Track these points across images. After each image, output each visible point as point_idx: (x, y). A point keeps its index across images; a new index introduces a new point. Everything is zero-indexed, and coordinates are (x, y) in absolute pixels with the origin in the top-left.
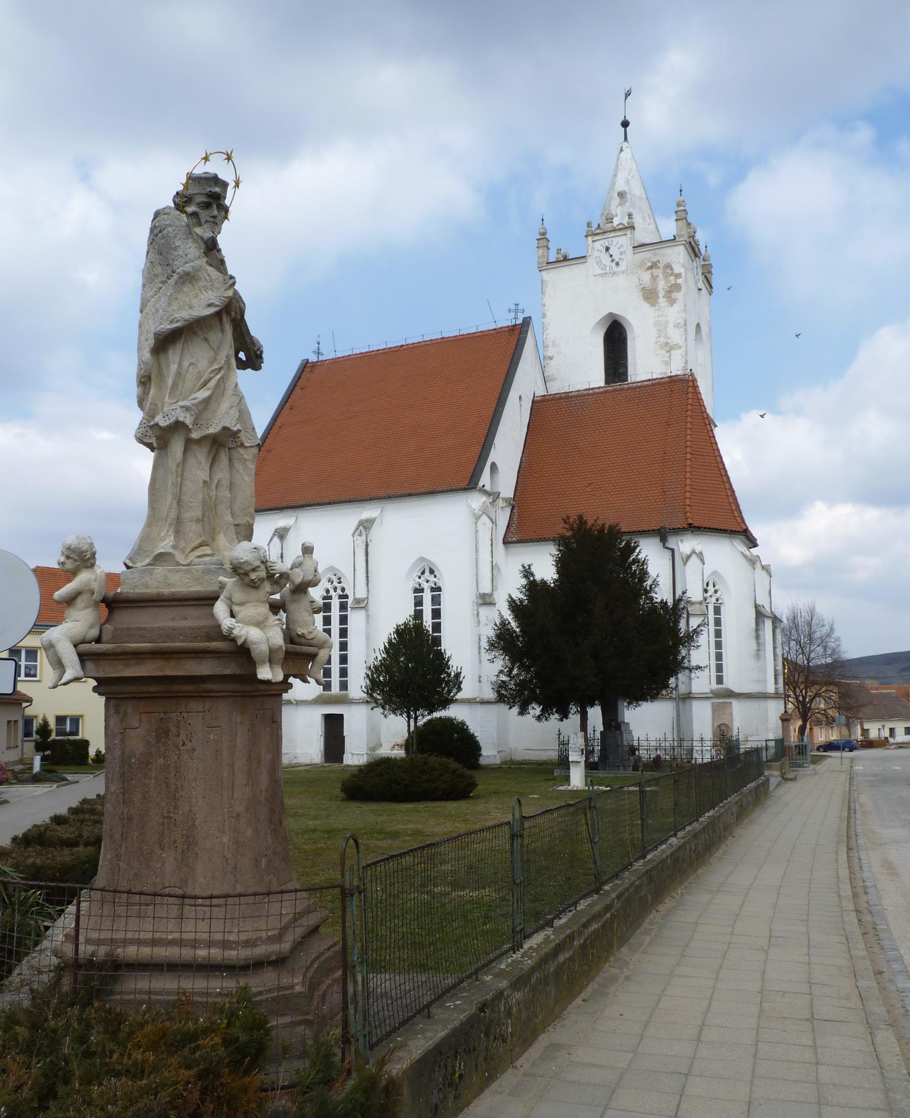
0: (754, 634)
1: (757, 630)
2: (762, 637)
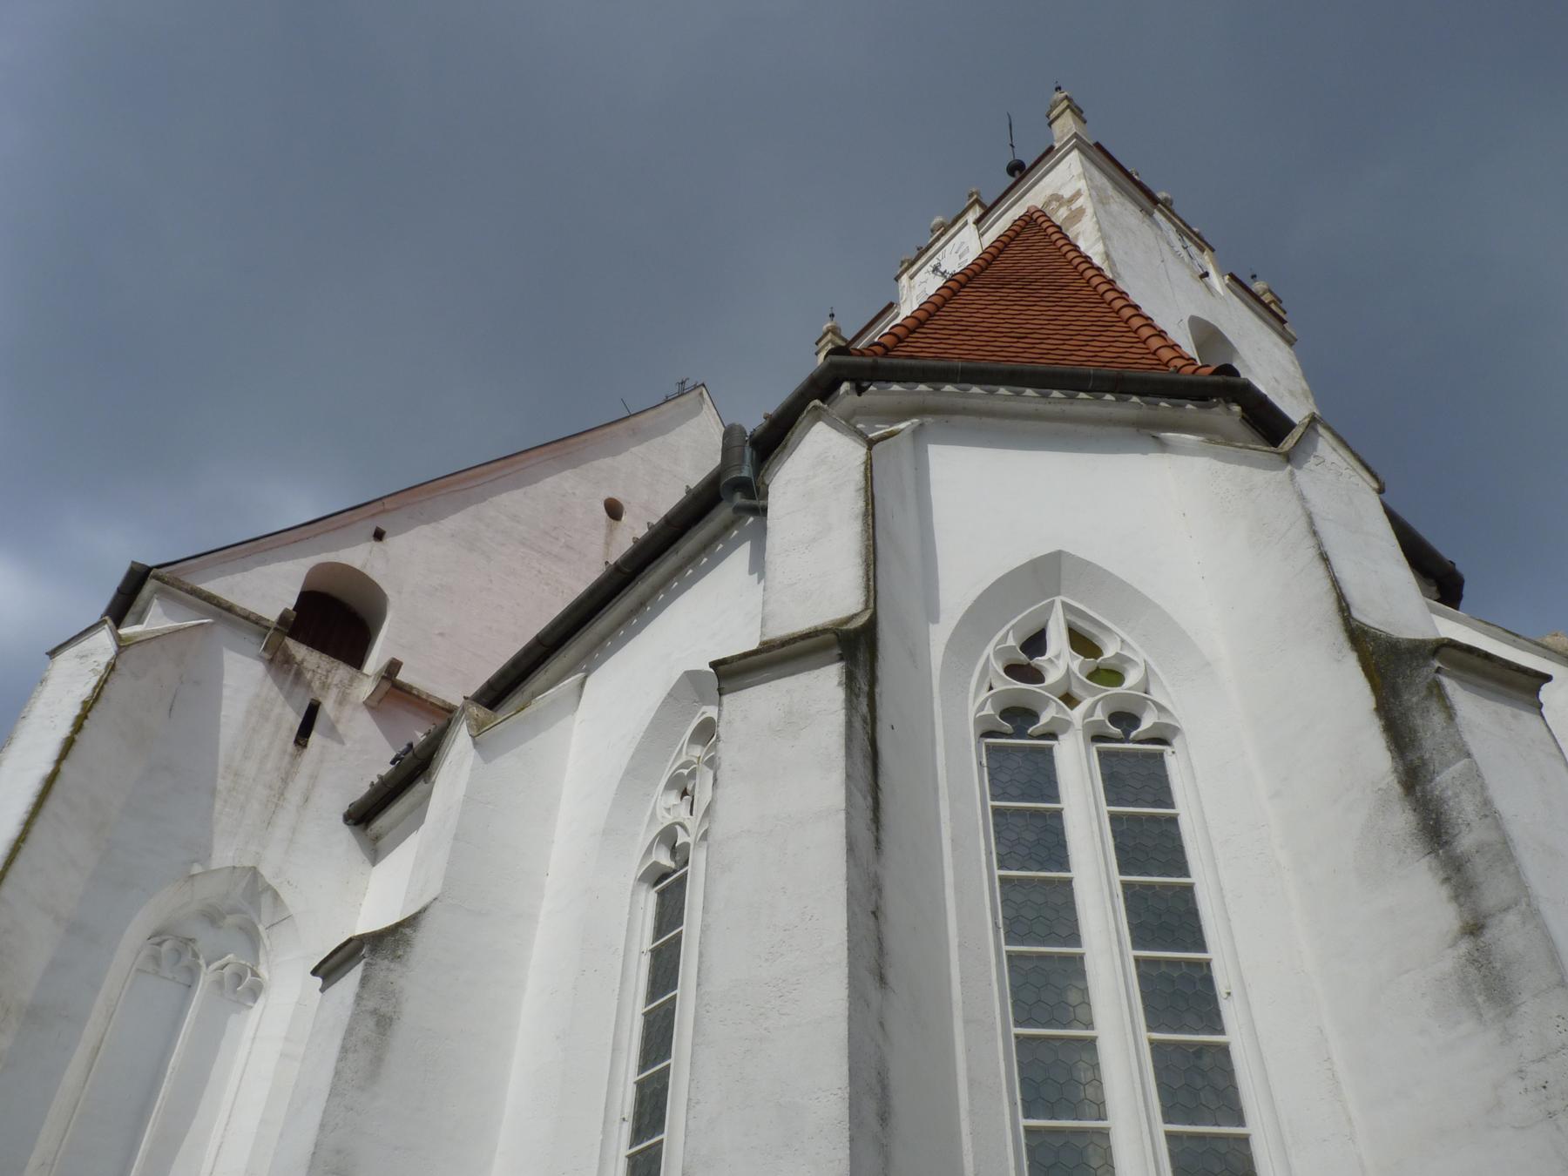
0: (1402, 819)
1: (1413, 776)
2: (1463, 808)
